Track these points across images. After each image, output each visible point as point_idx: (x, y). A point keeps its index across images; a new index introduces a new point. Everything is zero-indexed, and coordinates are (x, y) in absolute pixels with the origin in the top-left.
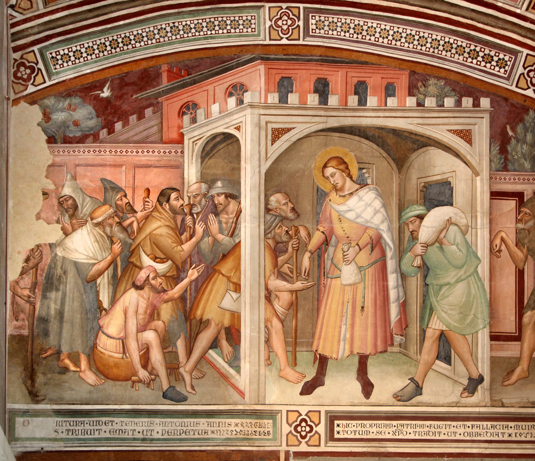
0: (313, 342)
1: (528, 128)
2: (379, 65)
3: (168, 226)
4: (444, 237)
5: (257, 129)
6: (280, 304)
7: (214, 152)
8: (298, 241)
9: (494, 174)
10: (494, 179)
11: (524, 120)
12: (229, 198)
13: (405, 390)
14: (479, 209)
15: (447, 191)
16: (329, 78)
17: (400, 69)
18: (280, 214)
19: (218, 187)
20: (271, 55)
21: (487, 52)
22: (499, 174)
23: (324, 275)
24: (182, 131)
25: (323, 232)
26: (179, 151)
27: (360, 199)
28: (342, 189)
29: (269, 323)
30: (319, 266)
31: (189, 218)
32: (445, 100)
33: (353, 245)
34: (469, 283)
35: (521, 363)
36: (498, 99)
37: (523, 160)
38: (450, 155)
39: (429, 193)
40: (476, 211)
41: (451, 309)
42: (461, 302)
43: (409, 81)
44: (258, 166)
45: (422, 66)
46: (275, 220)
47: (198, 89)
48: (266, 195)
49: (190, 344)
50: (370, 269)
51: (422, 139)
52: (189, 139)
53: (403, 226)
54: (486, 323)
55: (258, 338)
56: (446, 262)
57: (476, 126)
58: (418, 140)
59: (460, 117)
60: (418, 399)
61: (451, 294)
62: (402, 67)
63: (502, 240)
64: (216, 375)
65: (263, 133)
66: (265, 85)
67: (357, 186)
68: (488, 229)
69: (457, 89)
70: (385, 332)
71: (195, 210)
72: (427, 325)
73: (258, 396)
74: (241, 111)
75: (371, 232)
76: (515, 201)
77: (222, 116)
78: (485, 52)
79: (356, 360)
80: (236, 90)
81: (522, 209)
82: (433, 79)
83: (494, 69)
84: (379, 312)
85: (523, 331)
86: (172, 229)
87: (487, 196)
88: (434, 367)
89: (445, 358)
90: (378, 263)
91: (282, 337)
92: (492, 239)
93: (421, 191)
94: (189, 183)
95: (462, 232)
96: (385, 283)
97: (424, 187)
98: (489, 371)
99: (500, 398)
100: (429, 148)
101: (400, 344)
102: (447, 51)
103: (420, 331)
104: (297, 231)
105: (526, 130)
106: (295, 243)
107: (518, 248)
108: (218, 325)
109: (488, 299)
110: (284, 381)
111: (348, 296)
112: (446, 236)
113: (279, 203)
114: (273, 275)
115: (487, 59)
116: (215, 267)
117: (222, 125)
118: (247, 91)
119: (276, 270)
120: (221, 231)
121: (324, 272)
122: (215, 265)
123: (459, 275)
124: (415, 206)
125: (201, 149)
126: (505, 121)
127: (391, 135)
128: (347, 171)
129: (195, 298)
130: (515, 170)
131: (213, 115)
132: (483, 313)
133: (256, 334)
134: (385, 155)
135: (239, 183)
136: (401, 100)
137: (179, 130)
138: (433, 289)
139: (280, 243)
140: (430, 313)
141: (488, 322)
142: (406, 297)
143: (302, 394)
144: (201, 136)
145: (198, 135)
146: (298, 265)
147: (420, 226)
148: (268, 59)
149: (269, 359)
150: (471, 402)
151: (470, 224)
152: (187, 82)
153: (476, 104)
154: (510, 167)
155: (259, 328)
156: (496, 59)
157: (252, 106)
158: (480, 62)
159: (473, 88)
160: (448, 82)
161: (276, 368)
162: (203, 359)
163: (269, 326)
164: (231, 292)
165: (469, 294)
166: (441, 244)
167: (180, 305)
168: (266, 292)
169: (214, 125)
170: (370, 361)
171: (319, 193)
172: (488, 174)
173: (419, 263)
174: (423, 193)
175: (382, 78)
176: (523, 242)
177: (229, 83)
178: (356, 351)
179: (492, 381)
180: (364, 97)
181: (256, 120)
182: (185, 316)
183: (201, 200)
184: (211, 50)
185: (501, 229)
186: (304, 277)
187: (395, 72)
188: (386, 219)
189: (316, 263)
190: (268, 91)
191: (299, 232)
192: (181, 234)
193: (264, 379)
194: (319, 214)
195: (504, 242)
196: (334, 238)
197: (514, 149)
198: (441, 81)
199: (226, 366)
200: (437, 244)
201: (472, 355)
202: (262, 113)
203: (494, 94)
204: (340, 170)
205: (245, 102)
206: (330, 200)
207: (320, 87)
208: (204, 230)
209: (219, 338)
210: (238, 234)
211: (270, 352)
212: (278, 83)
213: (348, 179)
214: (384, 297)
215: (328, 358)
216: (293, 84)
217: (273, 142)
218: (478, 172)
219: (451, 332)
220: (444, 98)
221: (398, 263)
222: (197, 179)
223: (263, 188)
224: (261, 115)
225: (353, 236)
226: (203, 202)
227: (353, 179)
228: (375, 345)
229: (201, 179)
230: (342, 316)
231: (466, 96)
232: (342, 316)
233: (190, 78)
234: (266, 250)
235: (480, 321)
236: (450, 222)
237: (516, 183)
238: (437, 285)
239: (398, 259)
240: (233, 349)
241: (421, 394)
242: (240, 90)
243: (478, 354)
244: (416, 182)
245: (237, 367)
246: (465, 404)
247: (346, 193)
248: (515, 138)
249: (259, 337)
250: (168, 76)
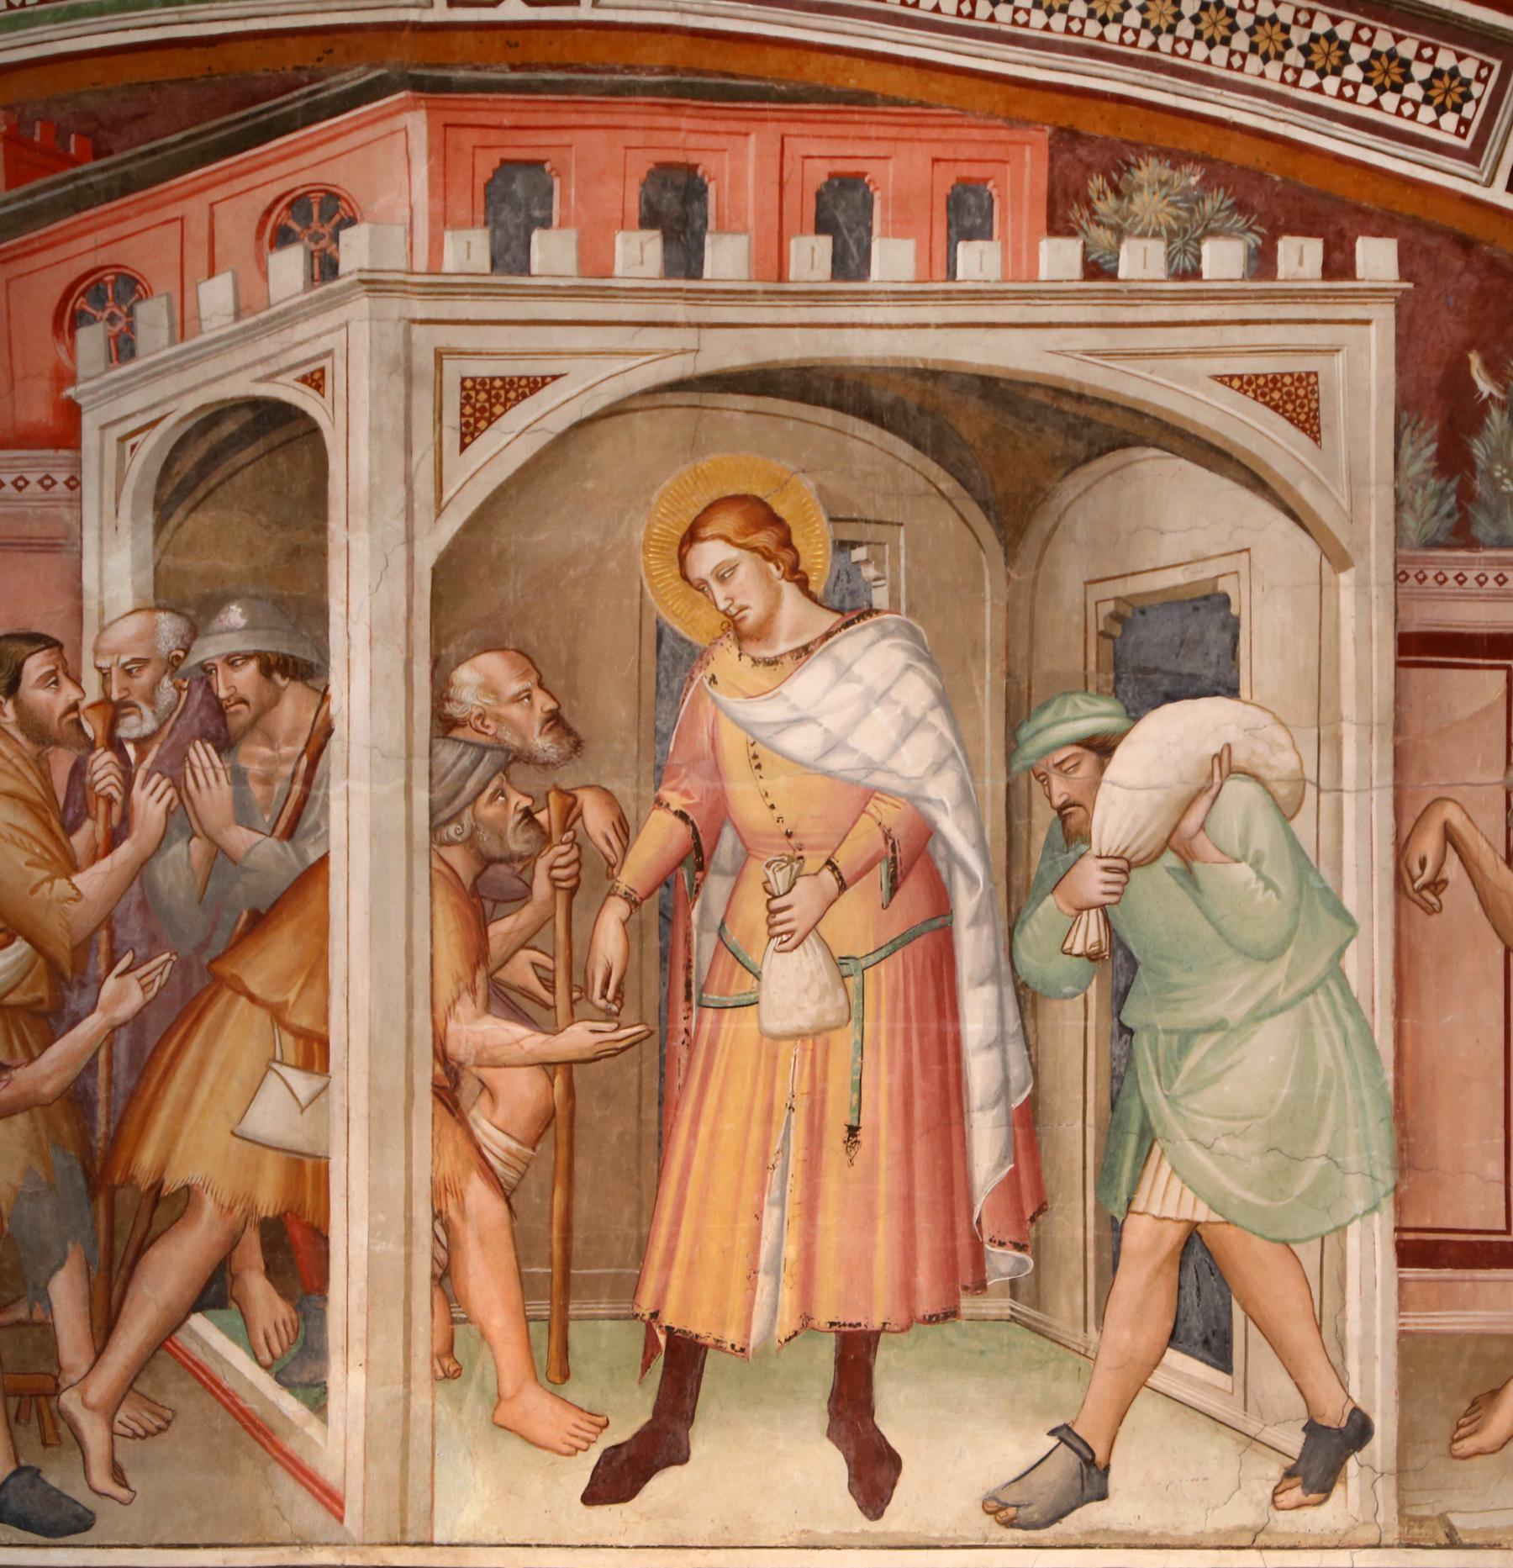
0: (639, 1279)
2: (920, 104)
3: (11, 795)
4: (1202, 827)
5: (399, 382)
6: (501, 1116)
7: (213, 481)
8: (574, 854)
9: (1412, 560)
10: (1412, 581)
12: (277, 677)
13: (1034, 1477)
14: (1348, 707)
15: (1215, 636)
16: (708, 165)
17: (1013, 122)
18: (499, 741)
19: (231, 630)
20: (453, 67)
21: (1383, 42)
22: (1433, 561)
23: (688, 997)
24: (70, 392)
25: (682, 815)
26: (61, 477)
27: (844, 673)
28: (763, 632)
29: (451, 1202)
30: (666, 957)
31: (103, 764)
32: (1208, 248)
33: (813, 862)
34: (1307, 1023)
36: (1432, 242)
38: (1226, 483)
39: (1139, 645)
40: (1338, 719)
41: (1231, 1134)
42: (1272, 1102)
43: (1051, 170)
44: (402, 537)
45: (1106, 105)
46: (475, 765)
47: (140, 213)
48: (436, 662)
49: (110, 1289)
50: (882, 968)
51: (1107, 417)
52: (103, 428)
53: (1023, 784)
54: (1382, 1189)
55: (402, 1263)
56: (1210, 932)
57: (1339, 359)
58: (1089, 422)
59: (1268, 322)
60: (1091, 1515)
61: (1230, 1067)
62: (1017, 111)
63: (1449, 836)
64: (222, 1420)
65: (424, 401)
66: (432, 195)
67: (829, 620)
68: (1390, 792)
69: (1257, 201)
70: (951, 1230)
71: (131, 727)
72: (1130, 1201)
73: (403, 1508)
74: (328, 309)
75: (889, 813)
76: (1502, 674)
77: (244, 330)
78: (1377, 45)
79: (825, 1353)
80: (306, 220)
82: (1153, 161)
83: (1413, 117)
84: (921, 1149)
86: (30, 806)
87: (1384, 651)
88: (1158, 1379)
89: (1206, 1342)
90: (920, 941)
91: (507, 1258)
92: (1405, 833)
93: (1102, 634)
94: (102, 614)
95: (1278, 807)
96: (949, 1027)
97: (1116, 617)
98: (1393, 1397)
99: (1440, 1509)
100: (1136, 453)
101: (1013, 1285)
102: (1211, 44)
103: (1097, 1226)
104: (571, 812)
106: (562, 861)
108: (231, 1209)
109: (1390, 1089)
110: (514, 1446)
111: (792, 1079)
112: (1210, 826)
113: (496, 693)
114: (467, 998)
115: (1386, 72)
116: (217, 967)
117: (246, 367)
118: (352, 222)
119: (481, 977)
120: (243, 814)
121: (688, 984)
122: (217, 959)
123: (1264, 989)
124: (1078, 699)
125: (156, 469)
126: (1460, 333)
127: (973, 403)
128: (786, 555)
129: (133, 1096)
131: (206, 326)
132: (1368, 1148)
133: (393, 1248)
134: (947, 484)
135: (321, 612)
136: (1017, 254)
137: (60, 389)
138: (1154, 1049)
139: (501, 861)
140: (1138, 1155)
141: (1390, 1184)
142: (1036, 1086)
143: (591, 1497)
144: (155, 414)
145: (143, 411)
146: (576, 952)
147: (1096, 785)
148: (444, 86)
149: (450, 1351)
150: (1316, 1530)
151: (1311, 773)
152: (90, 186)
153: (1338, 265)
154: (1482, 527)
155: (409, 1221)
156: (1421, 71)
157: (373, 285)
158: (1356, 87)
159: (1325, 196)
160: (1216, 172)
161: (482, 1390)
162: (162, 1353)
163: (453, 1213)
164: (286, 1072)
165: (1306, 1068)
166: (1187, 856)
167: (65, 1129)
168: (438, 1068)
169: (211, 368)
170: (885, 1359)
171: (665, 650)
172: (1391, 560)
173: (1093, 937)
174: (1108, 644)
175: (936, 160)
177: (277, 189)
178: (822, 1318)
180: (859, 242)
181: (393, 343)
182: (87, 1174)
183: (155, 685)
184: (196, 50)
185: (1445, 793)
186: (602, 1003)
187: (990, 135)
188: (953, 754)
189: (654, 943)
190: (442, 220)
191: (580, 814)
192: (72, 828)
193: (427, 1438)
194: (667, 737)
195: (1456, 848)
196: (728, 839)
198: (1186, 169)
199: (265, 1382)
200: (1170, 859)
201: (1319, 1328)
202: (420, 315)
203: (1415, 222)
204: (754, 549)
205: (343, 269)
206: (713, 679)
207: (669, 201)
208: (169, 812)
209: (236, 1263)
210: (317, 826)
211: (453, 1321)
212: (486, 186)
213: (789, 590)
214: (944, 1084)
215: (705, 1347)
216: (550, 191)
217: (468, 435)
218: (1344, 553)
219: (1232, 1231)
220: (1198, 241)
221: (1003, 941)
222: (138, 594)
223: (423, 631)
224: (414, 321)
225: (811, 829)
226: (167, 692)
227: (812, 588)
228: (908, 1291)
229: (156, 597)
230: (766, 1168)
231: (1293, 232)
232: (766, 1168)
233: (103, 169)
234: (440, 894)
235: (1354, 1181)
236: (1224, 765)
238: (1168, 1032)
239: (1003, 924)
240: (297, 1308)
241: (1103, 1496)
242: (326, 217)
243: (1344, 1320)
244: (1079, 598)
245: (311, 1385)
246: (1290, 1534)
247: (783, 647)
249: (408, 1257)
250: (6, 161)
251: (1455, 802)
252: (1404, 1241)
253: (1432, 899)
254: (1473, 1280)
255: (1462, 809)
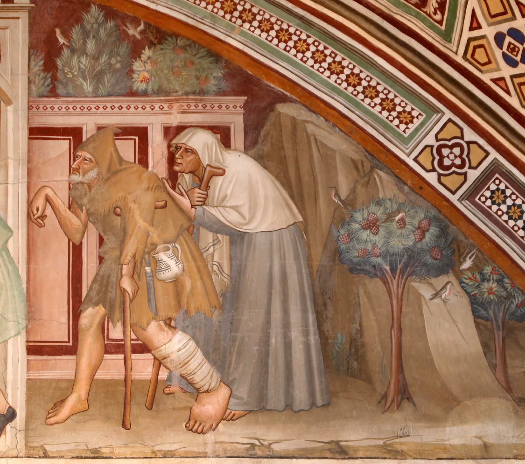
1: (89, 31)
9: (34, 102)
10: (35, 109)
11: (83, 20)
22: (42, 102)
35: (76, 388)
37: (81, 79)
54: (21, 327)
57: (8, 31)
63: (48, 199)
68: (26, 184)
76: (68, 141)
81: (79, 153)
85: (80, 338)
87: (24, 133)
92: (31, 198)
105: (86, 35)
107: (72, 212)
109: (25, 290)
130: (68, 95)
141: (25, 325)
154: (60, 90)
172: (27, 102)
176: (80, 202)
179: (29, 417)
197: (67, 64)
218: (9, 99)
235: (11, 324)
237: (70, 114)
243: (6, 375)
248: (68, 47)
251: (50, 187)
252: (29, 346)
253: (41, 222)
254: (55, 360)
255: (53, 190)
